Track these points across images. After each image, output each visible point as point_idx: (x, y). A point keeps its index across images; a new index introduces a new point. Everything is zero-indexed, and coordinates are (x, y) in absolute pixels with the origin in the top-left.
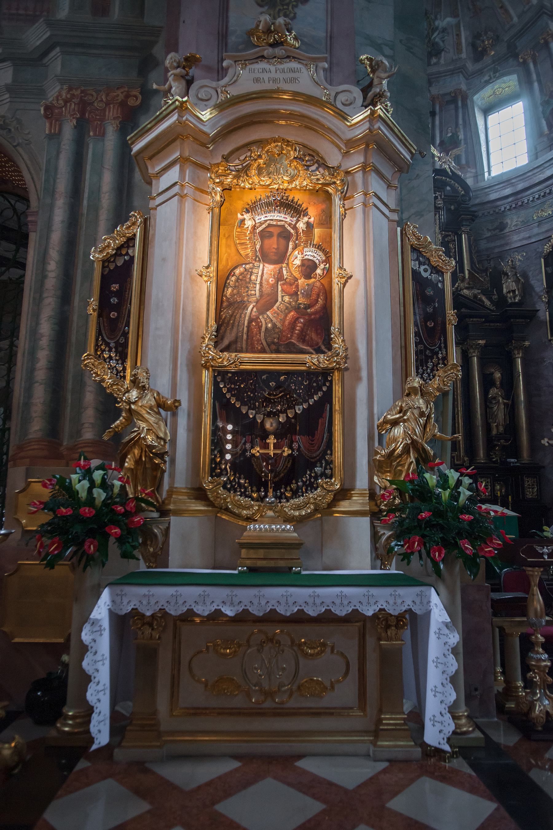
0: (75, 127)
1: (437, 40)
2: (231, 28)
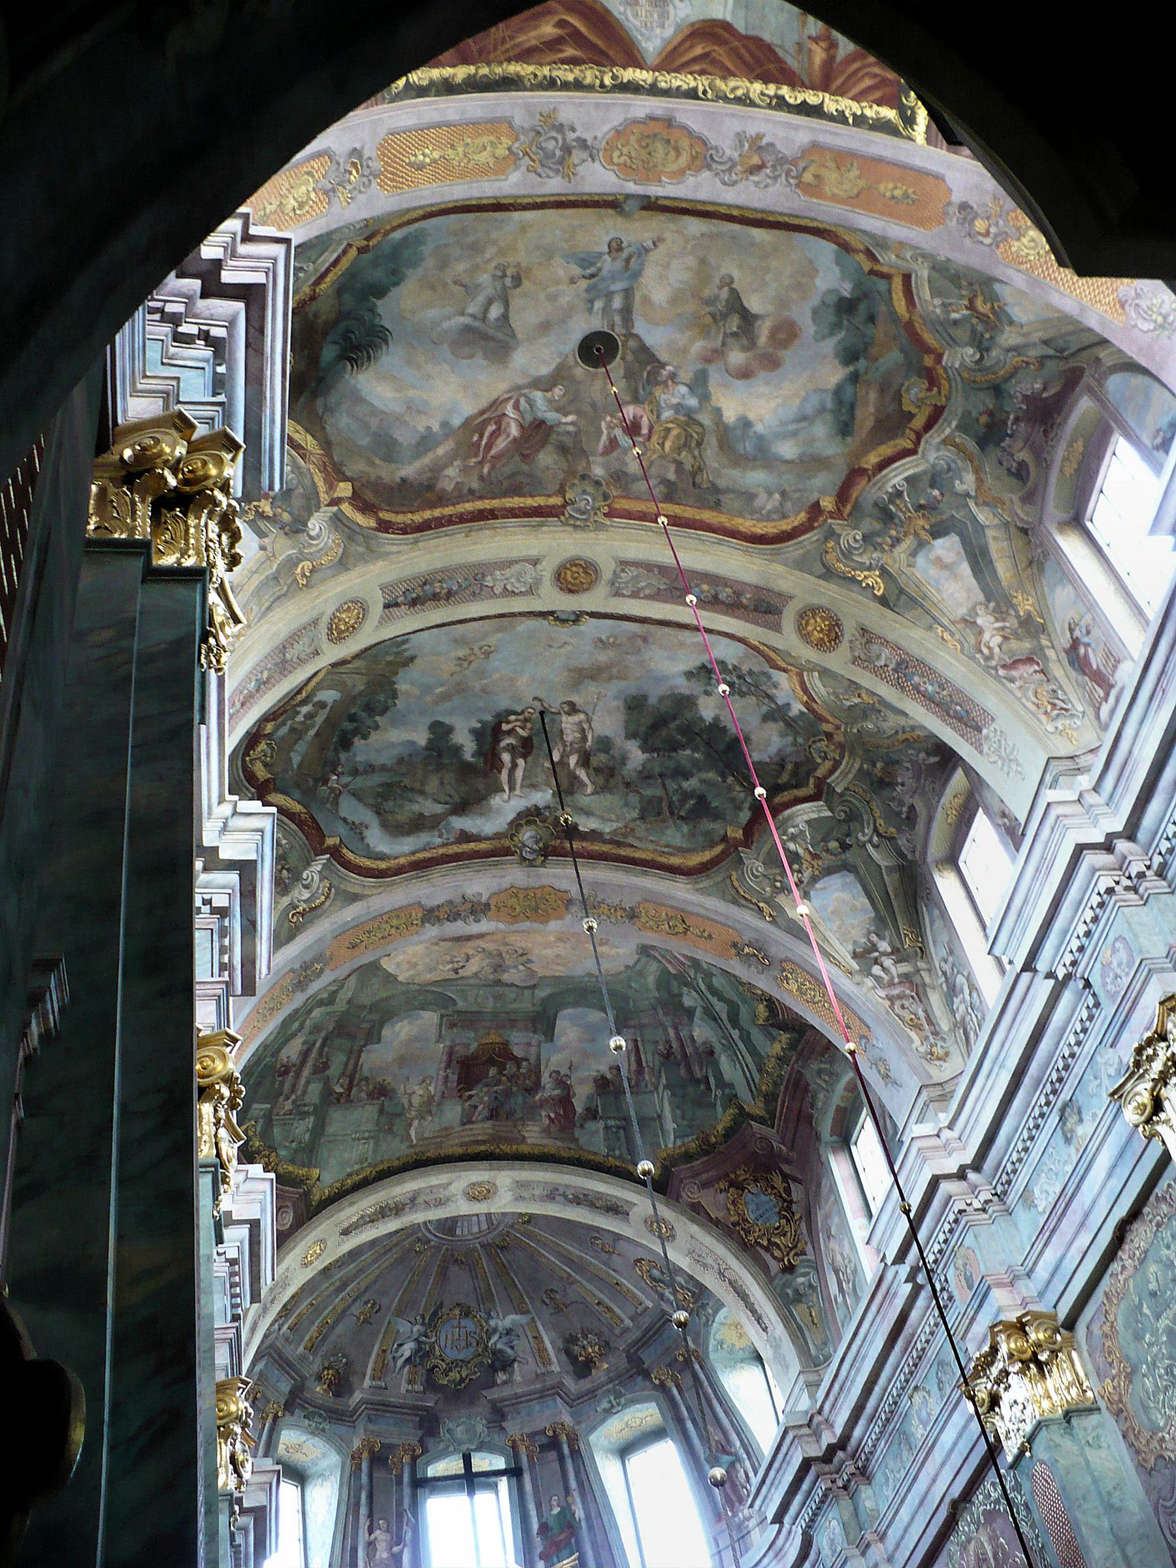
1: (499, 1346)
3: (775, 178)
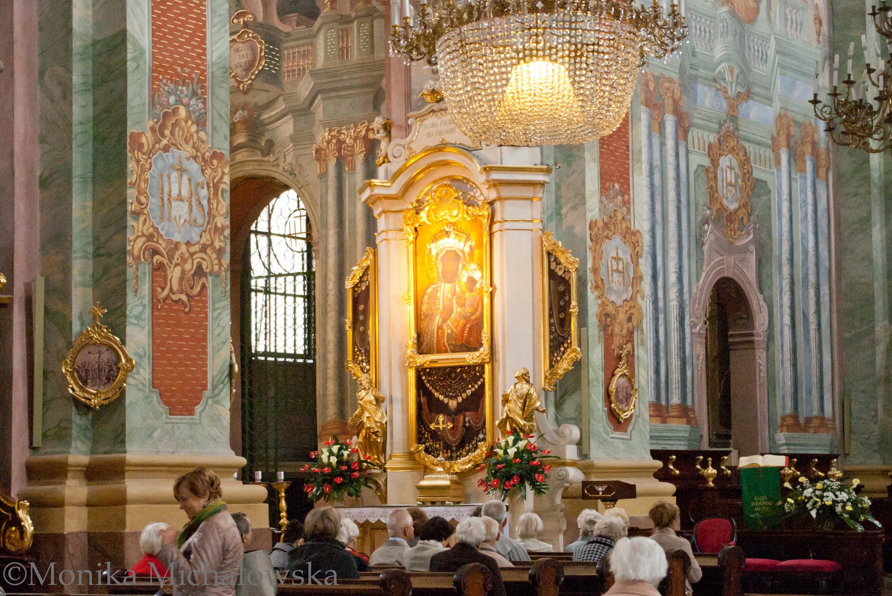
0: (336, 165)
2: (413, 87)
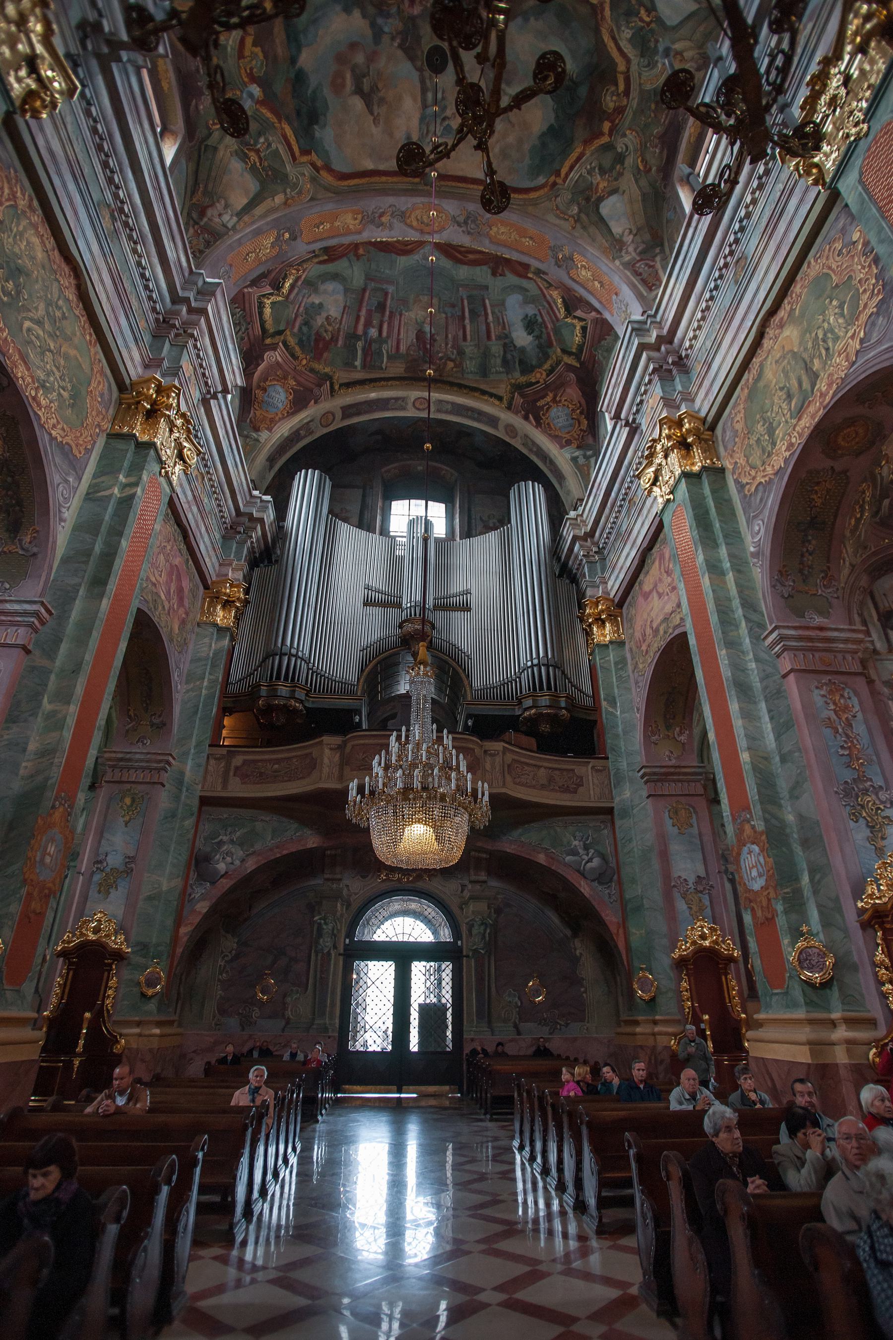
3: (373, 213)
